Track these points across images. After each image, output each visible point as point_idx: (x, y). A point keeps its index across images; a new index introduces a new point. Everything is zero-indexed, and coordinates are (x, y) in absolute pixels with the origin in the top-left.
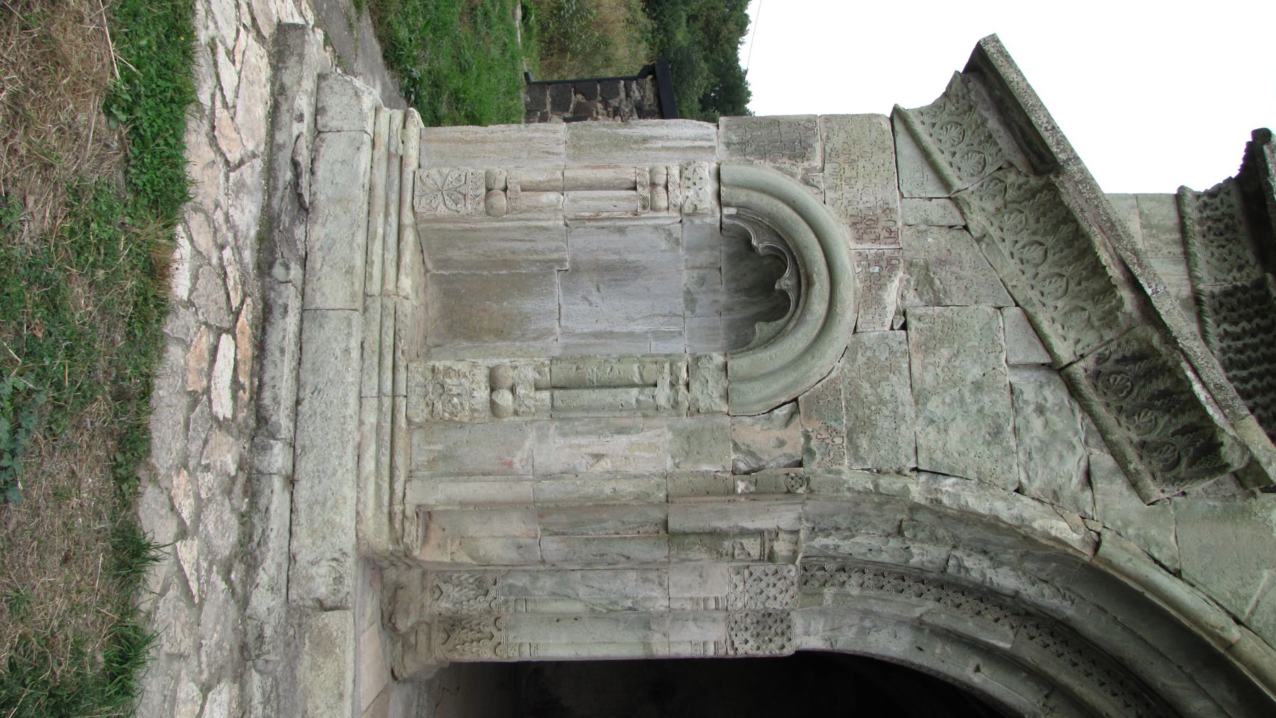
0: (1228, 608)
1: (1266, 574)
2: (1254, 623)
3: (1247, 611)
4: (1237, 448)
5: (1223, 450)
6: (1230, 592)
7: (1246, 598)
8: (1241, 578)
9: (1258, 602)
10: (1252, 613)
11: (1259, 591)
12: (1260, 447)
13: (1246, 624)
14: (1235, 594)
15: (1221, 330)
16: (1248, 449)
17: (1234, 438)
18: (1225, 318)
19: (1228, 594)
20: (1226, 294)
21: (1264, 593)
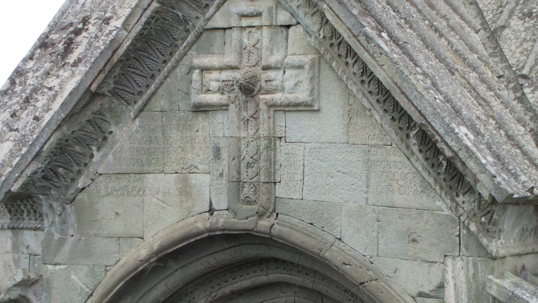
0: (86, 299)
1: (73, 277)
2: (92, 287)
3: (87, 290)
4: (10, 292)
5: (12, 298)
6: (79, 297)
7: (82, 289)
8: (74, 290)
9: (83, 284)
10: (88, 288)
11: (79, 282)
12: (9, 282)
13: (92, 291)
14: (80, 294)
15: (27, 218)
16: (9, 288)
17: (5, 294)
18: (21, 215)
19: (80, 298)
20: (10, 212)
21: (80, 280)
